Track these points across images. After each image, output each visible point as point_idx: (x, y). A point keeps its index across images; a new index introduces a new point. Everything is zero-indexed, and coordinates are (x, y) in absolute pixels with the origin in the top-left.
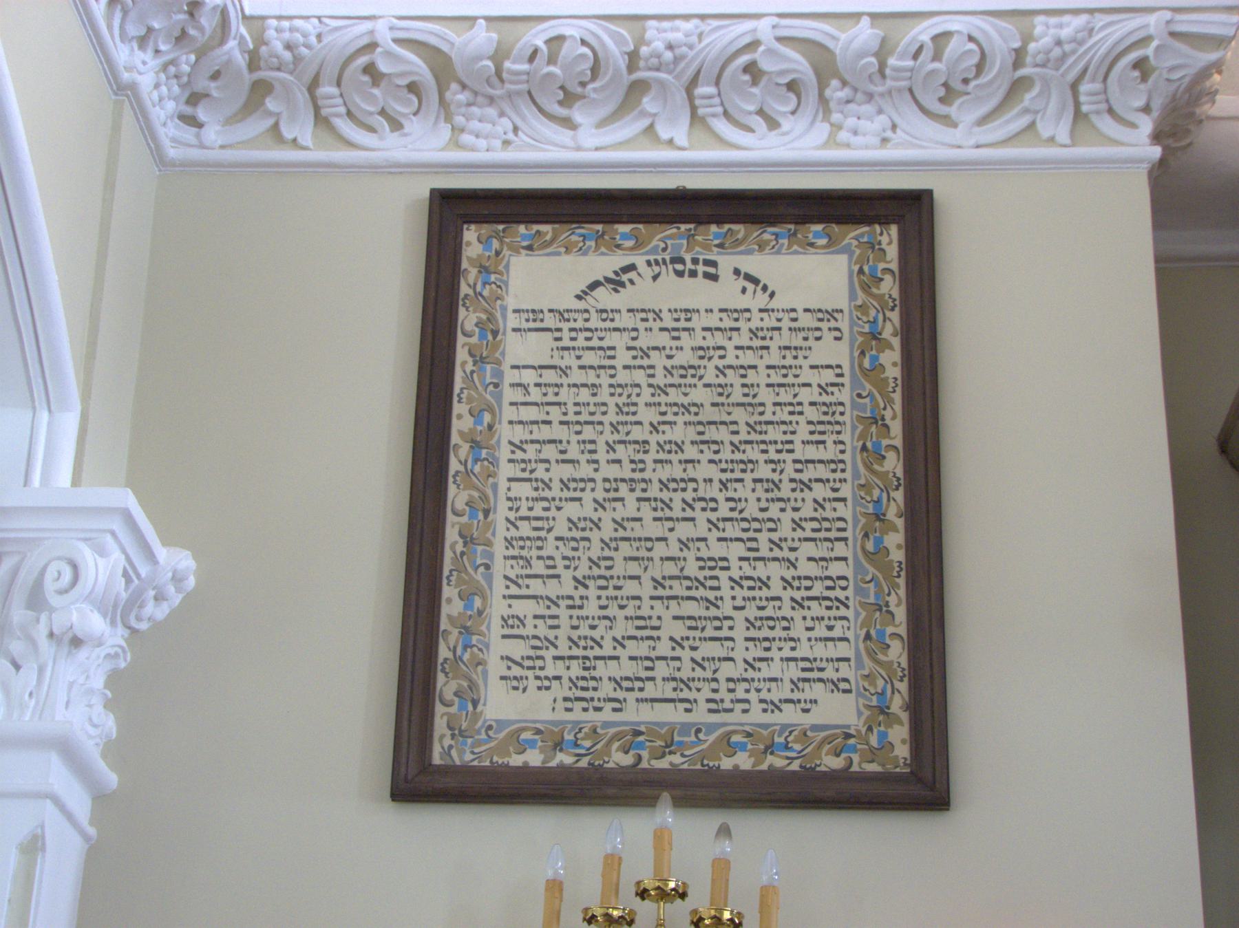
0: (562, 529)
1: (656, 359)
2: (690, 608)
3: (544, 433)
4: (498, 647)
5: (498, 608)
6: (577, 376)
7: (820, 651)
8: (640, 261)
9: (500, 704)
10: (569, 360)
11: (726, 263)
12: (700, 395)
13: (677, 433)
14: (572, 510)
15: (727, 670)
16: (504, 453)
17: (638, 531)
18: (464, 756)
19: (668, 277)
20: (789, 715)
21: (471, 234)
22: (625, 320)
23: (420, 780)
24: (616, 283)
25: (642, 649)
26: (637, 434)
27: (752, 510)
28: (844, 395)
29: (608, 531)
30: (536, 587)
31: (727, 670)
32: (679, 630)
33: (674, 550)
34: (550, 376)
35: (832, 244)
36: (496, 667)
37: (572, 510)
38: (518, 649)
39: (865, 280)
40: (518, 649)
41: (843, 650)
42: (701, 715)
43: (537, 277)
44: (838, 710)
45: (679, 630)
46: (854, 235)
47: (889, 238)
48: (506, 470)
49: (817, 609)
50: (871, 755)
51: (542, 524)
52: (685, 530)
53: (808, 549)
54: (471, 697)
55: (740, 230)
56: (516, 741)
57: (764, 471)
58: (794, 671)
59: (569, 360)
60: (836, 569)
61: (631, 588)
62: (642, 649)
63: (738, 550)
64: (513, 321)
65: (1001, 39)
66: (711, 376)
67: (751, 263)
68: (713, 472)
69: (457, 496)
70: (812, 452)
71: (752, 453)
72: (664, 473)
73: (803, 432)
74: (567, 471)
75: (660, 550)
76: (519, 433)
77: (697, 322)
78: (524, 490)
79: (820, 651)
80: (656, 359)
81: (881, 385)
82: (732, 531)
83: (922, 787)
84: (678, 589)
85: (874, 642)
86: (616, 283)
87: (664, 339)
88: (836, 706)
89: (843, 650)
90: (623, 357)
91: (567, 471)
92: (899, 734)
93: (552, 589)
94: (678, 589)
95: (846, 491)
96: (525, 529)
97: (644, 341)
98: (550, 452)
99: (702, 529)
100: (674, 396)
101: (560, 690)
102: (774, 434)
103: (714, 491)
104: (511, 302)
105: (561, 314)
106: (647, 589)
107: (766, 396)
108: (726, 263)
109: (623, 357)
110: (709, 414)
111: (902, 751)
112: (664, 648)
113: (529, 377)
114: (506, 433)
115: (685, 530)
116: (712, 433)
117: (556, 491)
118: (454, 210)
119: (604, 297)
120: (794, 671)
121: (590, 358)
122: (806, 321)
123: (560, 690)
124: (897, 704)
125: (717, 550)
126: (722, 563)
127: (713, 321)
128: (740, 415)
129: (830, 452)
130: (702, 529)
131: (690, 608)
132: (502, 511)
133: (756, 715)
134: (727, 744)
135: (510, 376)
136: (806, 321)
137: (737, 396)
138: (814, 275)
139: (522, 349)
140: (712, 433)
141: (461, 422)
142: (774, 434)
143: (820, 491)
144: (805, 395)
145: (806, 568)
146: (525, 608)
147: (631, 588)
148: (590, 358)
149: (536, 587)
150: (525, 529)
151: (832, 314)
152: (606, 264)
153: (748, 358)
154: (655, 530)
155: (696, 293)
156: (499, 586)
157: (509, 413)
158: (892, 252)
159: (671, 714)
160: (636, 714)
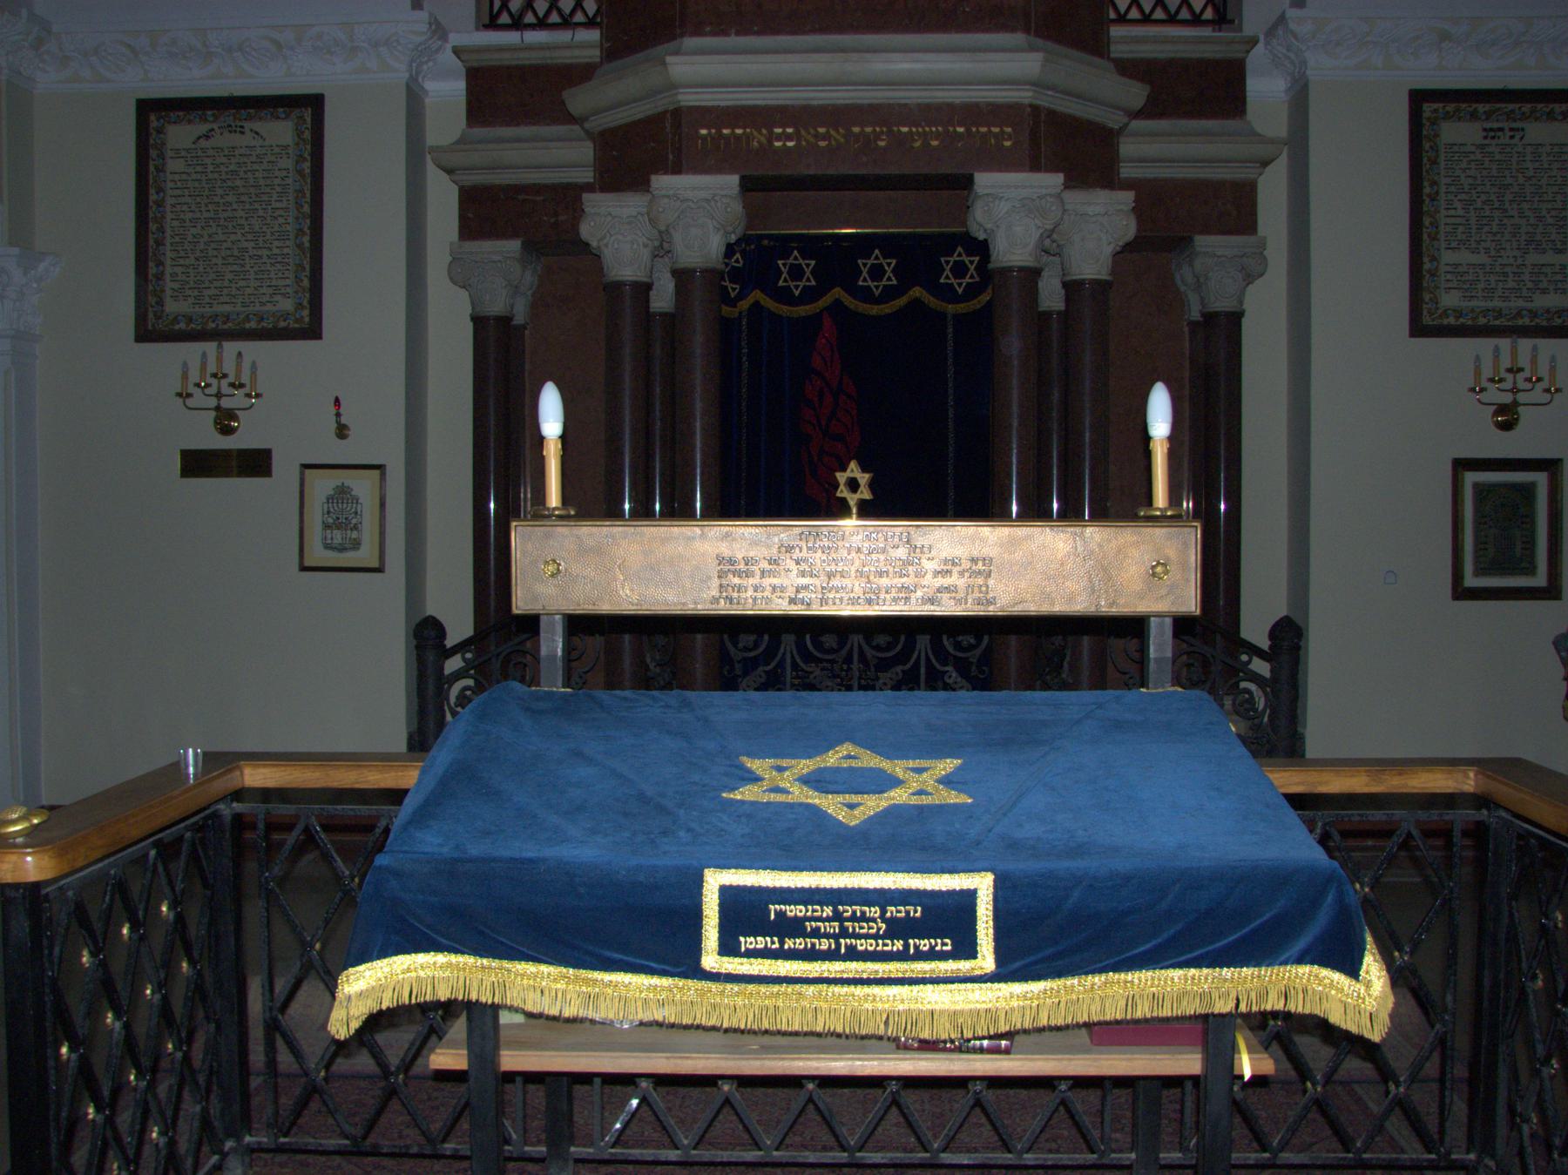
0: (190, 238)
1: (222, 168)
2: (235, 268)
3: (183, 200)
4: (169, 285)
5: (168, 270)
6: (194, 176)
7: (281, 283)
8: (215, 126)
9: (171, 307)
10: (190, 170)
12: (238, 183)
13: (230, 199)
14: (193, 231)
15: (249, 291)
16: (168, 208)
17: (216, 238)
19: (226, 134)
20: (269, 307)
21: (153, 117)
22: (211, 152)
25: (218, 284)
26: (216, 199)
27: (257, 228)
29: (206, 238)
30: (182, 262)
31: (249, 291)
32: (230, 276)
33: (229, 244)
34: (184, 177)
35: (287, 117)
36: (169, 292)
37: (193, 231)
38: (176, 286)
39: (299, 134)
40: (176, 286)
41: (288, 282)
42: (239, 308)
43: (179, 135)
44: (287, 305)
45: (230, 276)
46: (297, 112)
48: (169, 216)
49: (279, 266)
50: (297, 321)
52: (233, 237)
53: (276, 243)
54: (160, 303)
56: (176, 320)
57: (261, 213)
58: (271, 291)
59: (190, 170)
60: (286, 251)
61: (214, 260)
62: (218, 284)
63: (252, 244)
64: (169, 154)
67: (257, 126)
68: (242, 213)
70: (278, 205)
71: (257, 206)
72: (226, 215)
73: (275, 197)
74: (190, 215)
75: (225, 245)
76: (173, 201)
78: (176, 223)
79: (281, 283)
80: (222, 168)
82: (250, 237)
84: (231, 260)
85: (298, 280)
86: (207, 137)
87: (224, 160)
89: (288, 282)
90: (211, 168)
91: (190, 215)
92: (306, 313)
93: (187, 262)
94: (231, 260)
95: (290, 220)
96: (177, 239)
97: (218, 161)
98: (185, 208)
99: (239, 236)
100: (229, 183)
101: (191, 300)
102: (265, 198)
103: (243, 222)
104: (169, 146)
105: (187, 150)
106: (220, 261)
107: (262, 182)
108: (248, 125)
109: (211, 168)
110: (242, 190)
111: (307, 319)
112: (226, 283)
113: (177, 177)
114: (170, 201)
115: (233, 237)
116: (243, 198)
118: (149, 109)
119: (203, 143)
120: (271, 291)
121: (199, 169)
122: (277, 150)
123: (191, 300)
124: (305, 303)
125: (246, 244)
126: (245, 250)
127: (243, 151)
128: (252, 190)
129: (283, 205)
130: (239, 236)
131: (235, 268)
132: (169, 232)
133: (258, 308)
134: (247, 319)
135: (170, 177)
136: (277, 150)
137: (252, 181)
138: (281, 131)
139: (174, 165)
140: (243, 198)
142: (265, 198)
143: (281, 220)
144: (277, 181)
145: (276, 251)
146: (177, 270)
147: (214, 260)
148: (199, 169)
149: (182, 262)
150: (177, 239)
152: (204, 128)
153: (256, 167)
154: (222, 237)
156: (168, 262)
157: (170, 192)
158: (309, 120)
159: (227, 308)
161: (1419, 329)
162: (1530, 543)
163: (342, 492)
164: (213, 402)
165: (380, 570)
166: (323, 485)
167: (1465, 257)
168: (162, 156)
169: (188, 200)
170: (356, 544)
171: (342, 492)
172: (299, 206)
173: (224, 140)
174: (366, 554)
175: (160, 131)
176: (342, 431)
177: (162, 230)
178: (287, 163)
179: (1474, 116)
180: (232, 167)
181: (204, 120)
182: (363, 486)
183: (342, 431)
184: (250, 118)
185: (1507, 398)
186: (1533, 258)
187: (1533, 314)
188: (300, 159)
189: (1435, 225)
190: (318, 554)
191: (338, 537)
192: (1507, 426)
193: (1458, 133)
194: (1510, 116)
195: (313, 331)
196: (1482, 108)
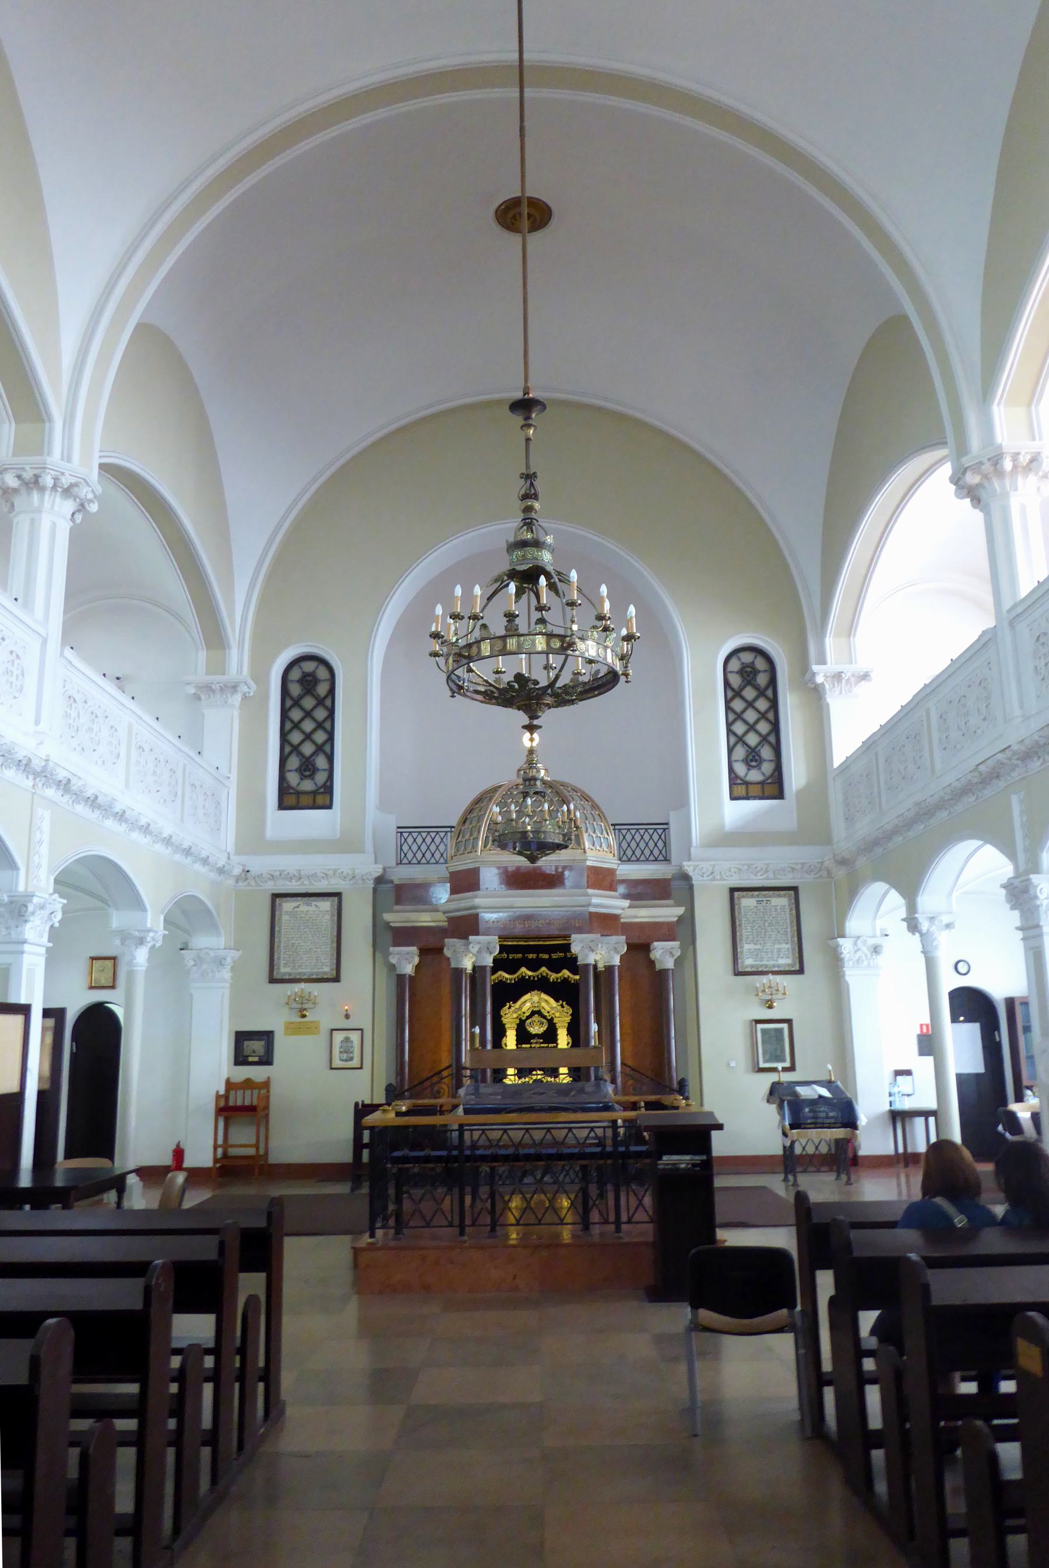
4: (282, 962)
9: (283, 970)
18: (279, 977)
23: (272, 980)
39: (332, 906)
43: (288, 905)
44: (327, 969)
46: (332, 898)
47: (336, 899)
54: (279, 968)
65: (350, 873)
69: (276, 940)
83: (337, 979)
88: (327, 968)
118: (275, 896)
138: (326, 905)
139: (285, 917)
141: (277, 929)
152: (296, 904)
160: (301, 970)
161: (738, 973)
162: (783, 1050)
163: (347, 1039)
164: (300, 1006)
165: (361, 1068)
166: (339, 1037)
167: (751, 946)
168: (281, 914)
170: (351, 1059)
171: (347, 1039)
173: (303, 908)
174: (355, 1063)
175: (280, 905)
176: (347, 1016)
178: (328, 917)
179: (752, 896)
182: (355, 1037)
183: (347, 1016)
185: (769, 997)
186: (777, 946)
187: (778, 966)
188: (333, 915)
189: (741, 935)
190: (337, 1063)
191: (345, 1056)
192: (770, 1007)
193: (747, 903)
194: (765, 896)
195: (337, 979)
196: (756, 893)
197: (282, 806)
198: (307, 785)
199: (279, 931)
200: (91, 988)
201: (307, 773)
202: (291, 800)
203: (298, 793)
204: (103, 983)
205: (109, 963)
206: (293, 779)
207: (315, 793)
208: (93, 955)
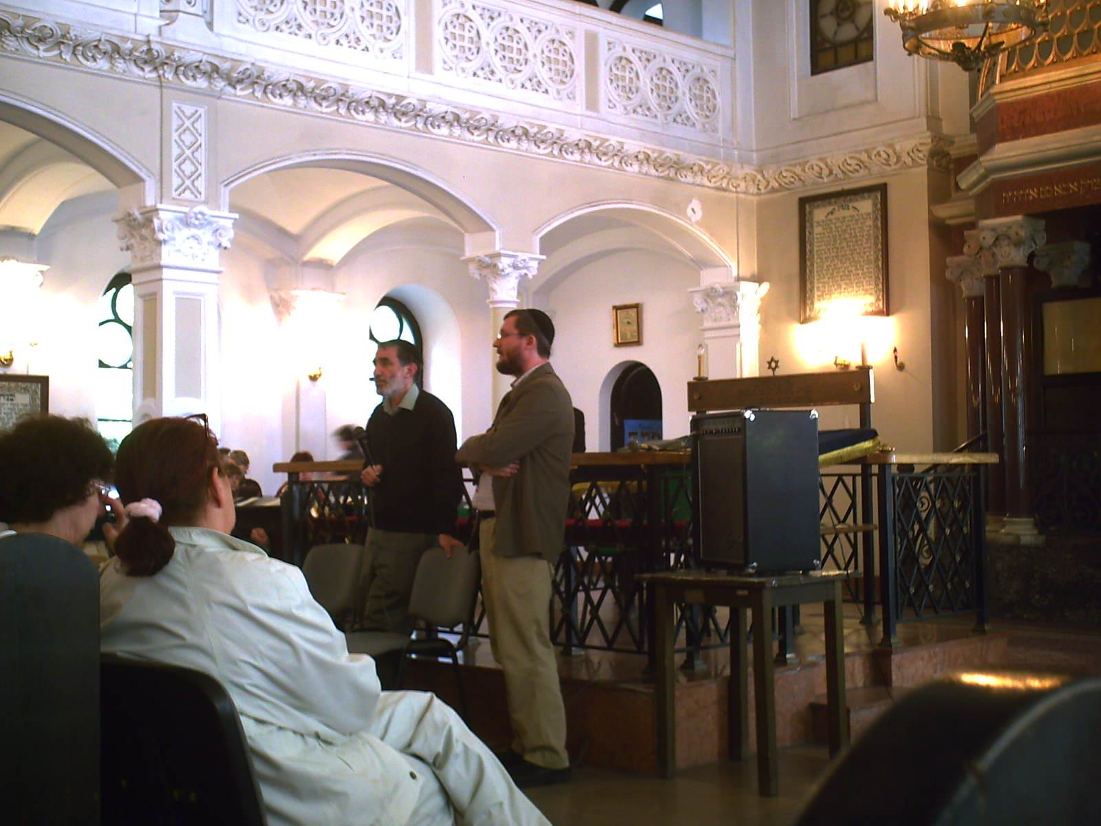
11: (850, 205)
21: (807, 206)
24: (832, 213)
28: (871, 232)
35: (869, 197)
36: (816, 297)
39: (875, 205)
43: (819, 214)
46: (873, 194)
48: (815, 257)
51: (822, 267)
53: (866, 266)
55: (853, 197)
64: (815, 224)
66: (849, 231)
67: (855, 204)
77: (846, 219)
81: (878, 229)
86: (832, 213)
87: (840, 224)
90: (834, 229)
93: (825, 280)
97: (837, 225)
105: (823, 221)
109: (834, 229)
110: (849, 239)
114: (815, 249)
117: (824, 260)
119: (830, 216)
125: (850, 269)
138: (866, 206)
139: (817, 230)
146: (820, 285)
151: (869, 214)
152: (830, 209)
155: (846, 213)
168: (812, 226)
169: (824, 247)
172: (876, 244)
173: (841, 213)
175: (811, 213)
177: (812, 265)
178: (870, 222)
180: (844, 227)
181: (830, 204)
184: (851, 201)
197: (818, 66)
198: (848, 32)
199: (811, 252)
200: (618, 345)
201: (846, 14)
202: (828, 58)
203: (836, 47)
204: (629, 338)
205: (633, 312)
206: (828, 26)
207: (855, 42)
208: (618, 304)
